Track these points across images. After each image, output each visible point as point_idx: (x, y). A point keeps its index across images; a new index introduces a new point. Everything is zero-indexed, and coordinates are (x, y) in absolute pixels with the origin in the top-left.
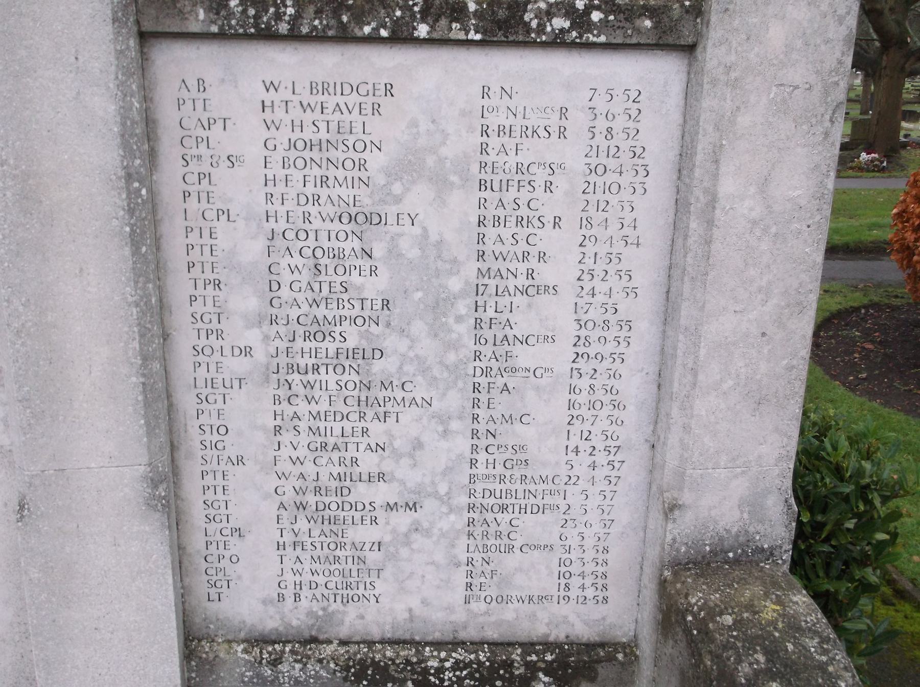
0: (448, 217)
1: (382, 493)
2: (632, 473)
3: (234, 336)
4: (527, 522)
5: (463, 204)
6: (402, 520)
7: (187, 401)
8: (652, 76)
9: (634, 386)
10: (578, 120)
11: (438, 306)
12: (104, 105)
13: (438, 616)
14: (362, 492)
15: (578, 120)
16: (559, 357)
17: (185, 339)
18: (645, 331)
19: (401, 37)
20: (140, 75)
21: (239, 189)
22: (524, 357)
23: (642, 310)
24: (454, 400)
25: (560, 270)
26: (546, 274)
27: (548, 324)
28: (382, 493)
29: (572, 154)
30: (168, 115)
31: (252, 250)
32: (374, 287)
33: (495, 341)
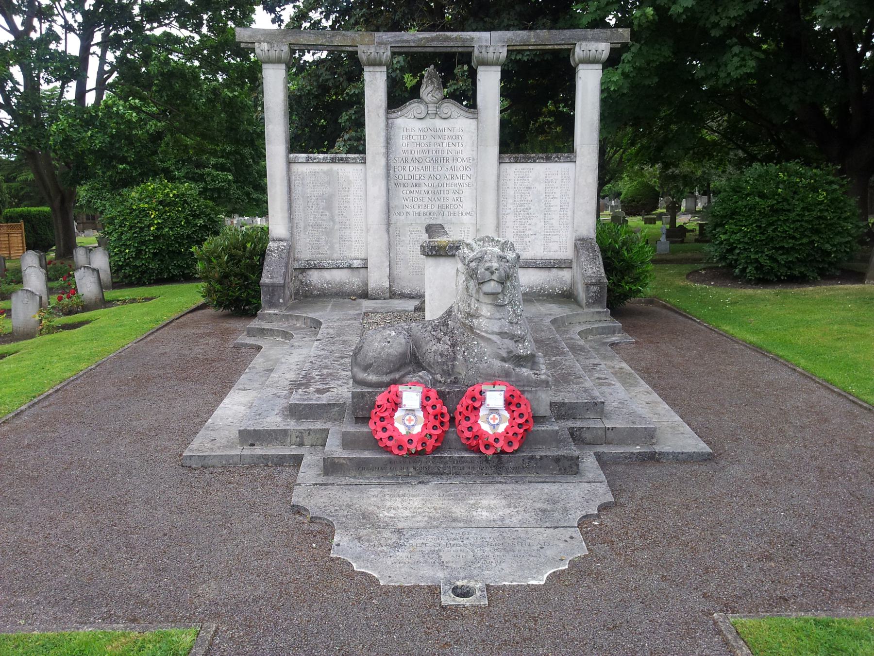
0: (540, 187)
1: (530, 232)
2: (570, 229)
3: (510, 205)
4: (554, 237)
5: (543, 185)
6: (533, 237)
7: (501, 217)
8: (572, 164)
9: (569, 213)
10: (560, 173)
11: (539, 201)
12: (495, 172)
13: (539, 254)
14: (527, 232)
15: (560, 173)
16: (558, 208)
17: (501, 207)
18: (571, 203)
19: (535, 162)
20: (499, 167)
21: (510, 184)
22: (552, 209)
23: (570, 201)
24: (542, 216)
25: (558, 195)
26: (556, 196)
27: (556, 203)
28: (530, 232)
29: (559, 177)
30: (501, 174)
31: (512, 193)
32: (530, 198)
33: (548, 206)
